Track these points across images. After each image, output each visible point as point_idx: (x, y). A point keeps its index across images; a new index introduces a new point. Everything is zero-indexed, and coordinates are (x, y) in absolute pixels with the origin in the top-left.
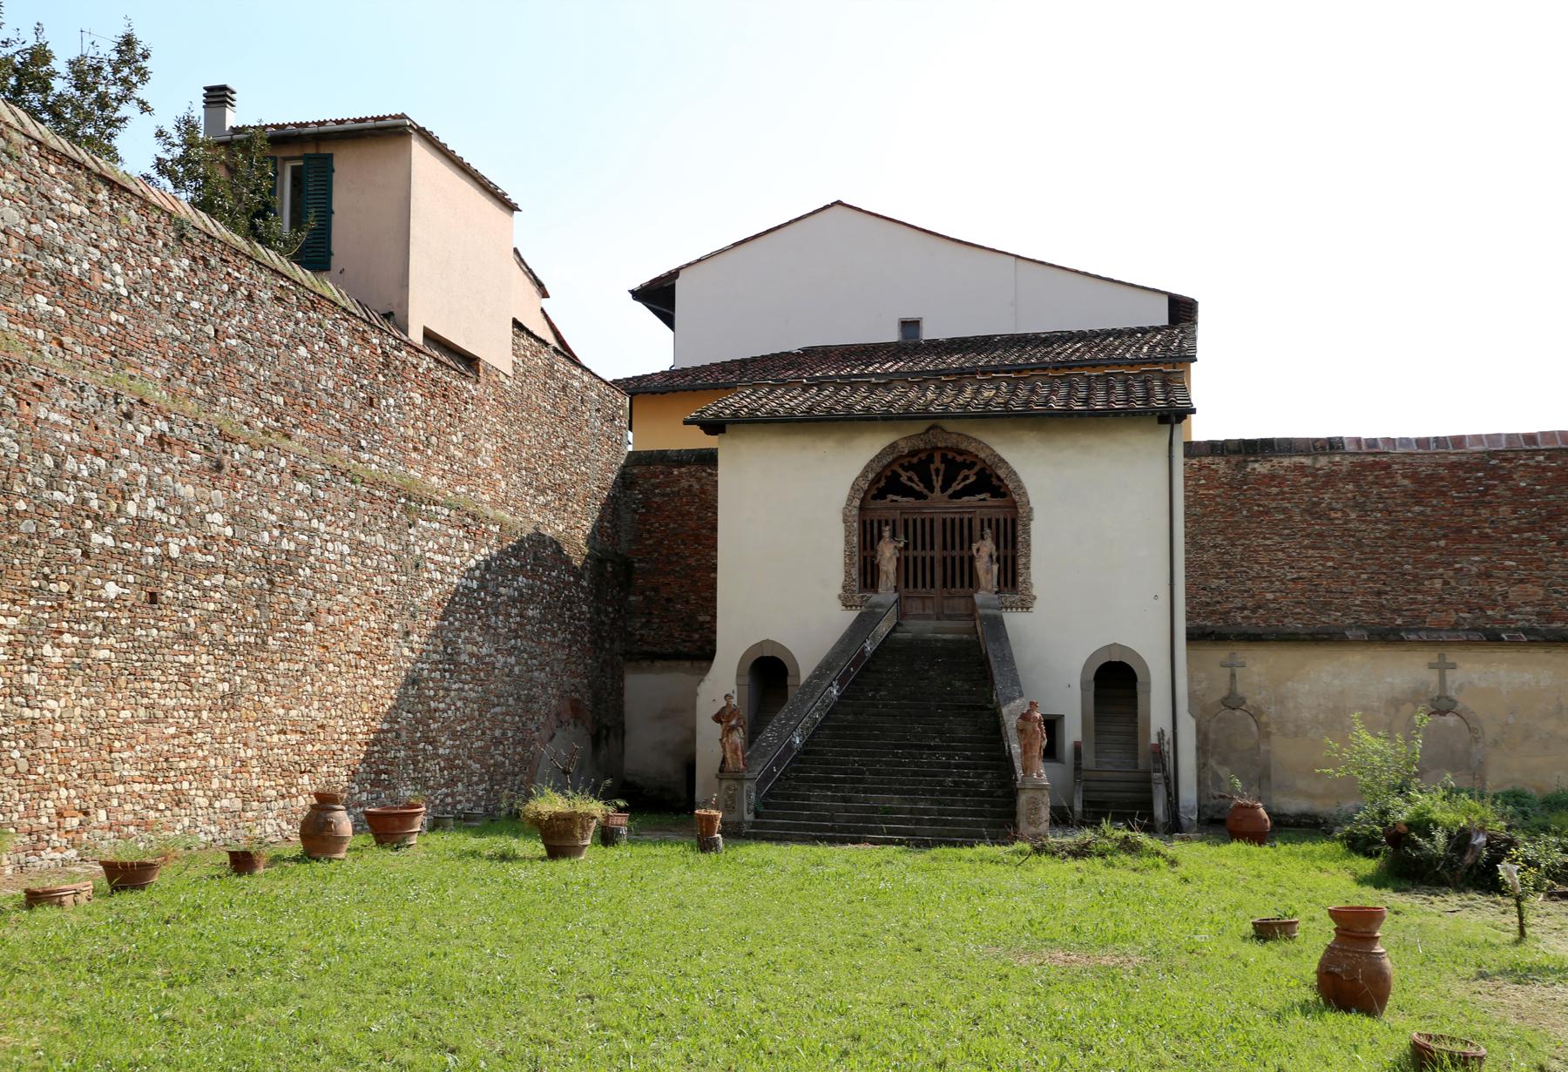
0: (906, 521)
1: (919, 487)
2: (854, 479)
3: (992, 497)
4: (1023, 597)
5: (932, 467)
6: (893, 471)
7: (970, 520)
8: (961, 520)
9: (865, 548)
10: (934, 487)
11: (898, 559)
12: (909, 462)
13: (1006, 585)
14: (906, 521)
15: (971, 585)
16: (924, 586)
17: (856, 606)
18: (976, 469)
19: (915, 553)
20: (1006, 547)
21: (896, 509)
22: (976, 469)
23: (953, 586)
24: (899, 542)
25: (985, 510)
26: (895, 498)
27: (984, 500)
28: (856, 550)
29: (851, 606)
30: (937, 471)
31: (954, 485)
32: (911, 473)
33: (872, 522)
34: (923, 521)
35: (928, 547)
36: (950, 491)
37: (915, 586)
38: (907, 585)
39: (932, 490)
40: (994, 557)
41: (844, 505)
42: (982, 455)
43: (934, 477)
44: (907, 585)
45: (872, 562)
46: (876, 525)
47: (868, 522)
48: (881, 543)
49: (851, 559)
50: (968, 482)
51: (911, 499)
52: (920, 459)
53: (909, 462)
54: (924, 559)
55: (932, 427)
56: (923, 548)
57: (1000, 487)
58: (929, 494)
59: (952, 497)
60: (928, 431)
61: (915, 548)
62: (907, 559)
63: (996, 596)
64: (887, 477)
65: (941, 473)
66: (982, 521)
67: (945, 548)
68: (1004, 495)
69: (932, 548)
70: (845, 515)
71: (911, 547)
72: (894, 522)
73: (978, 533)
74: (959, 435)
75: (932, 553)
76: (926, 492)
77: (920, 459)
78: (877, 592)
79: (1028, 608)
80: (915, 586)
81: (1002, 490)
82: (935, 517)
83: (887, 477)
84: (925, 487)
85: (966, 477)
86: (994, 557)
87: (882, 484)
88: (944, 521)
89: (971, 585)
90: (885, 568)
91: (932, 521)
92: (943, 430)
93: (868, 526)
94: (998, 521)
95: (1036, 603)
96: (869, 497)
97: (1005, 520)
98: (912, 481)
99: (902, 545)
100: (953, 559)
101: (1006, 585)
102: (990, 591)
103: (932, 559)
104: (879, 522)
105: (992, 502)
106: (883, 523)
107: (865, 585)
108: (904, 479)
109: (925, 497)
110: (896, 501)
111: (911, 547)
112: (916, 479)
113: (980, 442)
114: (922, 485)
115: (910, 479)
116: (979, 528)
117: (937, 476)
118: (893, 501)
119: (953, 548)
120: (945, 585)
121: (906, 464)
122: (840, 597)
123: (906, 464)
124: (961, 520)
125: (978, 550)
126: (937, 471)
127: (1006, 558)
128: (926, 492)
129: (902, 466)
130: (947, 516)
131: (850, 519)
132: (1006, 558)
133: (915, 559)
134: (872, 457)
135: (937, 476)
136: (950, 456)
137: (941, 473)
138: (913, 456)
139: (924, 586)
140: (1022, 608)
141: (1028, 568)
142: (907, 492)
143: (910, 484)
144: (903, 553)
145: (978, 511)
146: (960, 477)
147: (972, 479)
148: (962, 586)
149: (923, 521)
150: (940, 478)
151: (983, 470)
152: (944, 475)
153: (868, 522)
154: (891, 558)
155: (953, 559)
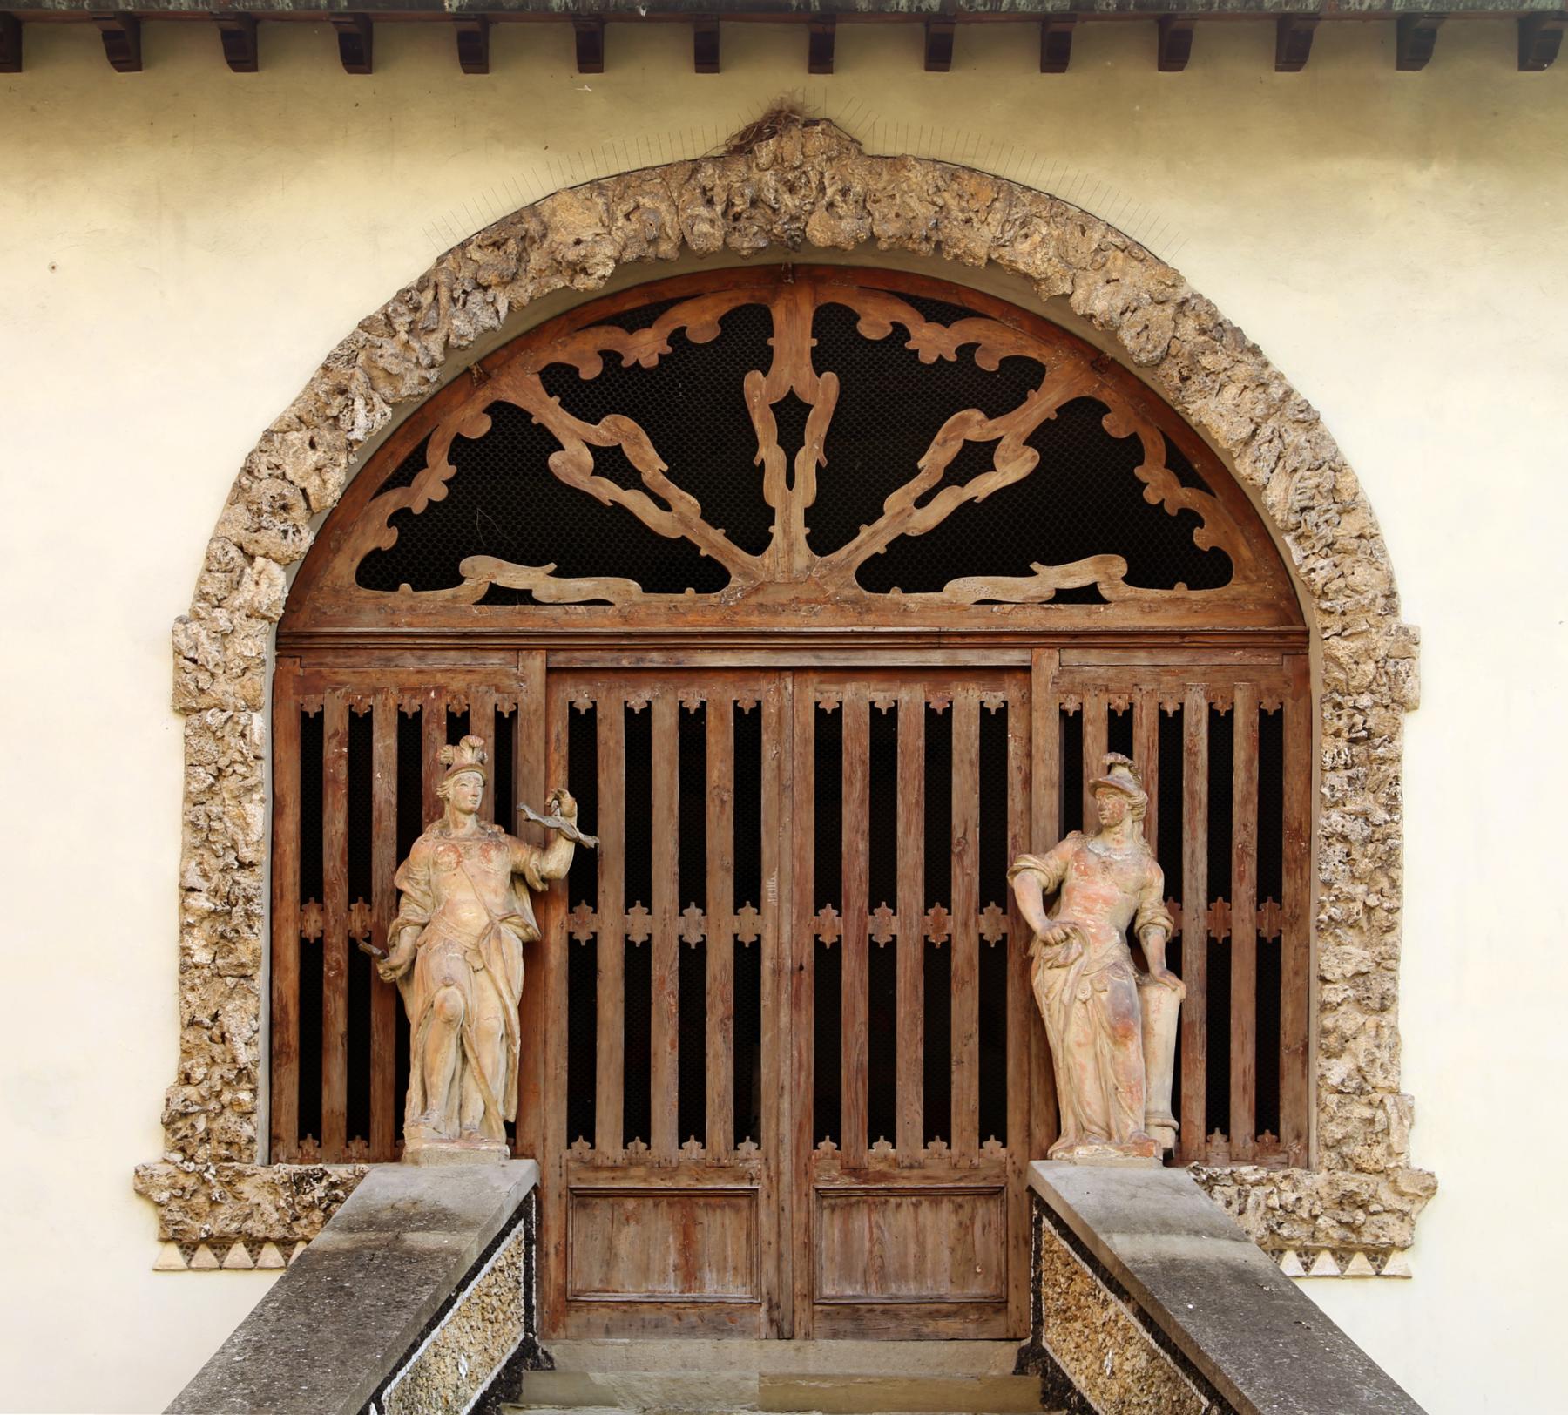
0: (583, 726)
2: (253, 440)
3: (1129, 579)
4: (1351, 1182)
5: (759, 391)
6: (500, 411)
7: (993, 725)
8: (938, 725)
9: (312, 887)
10: (769, 515)
11: (532, 951)
12: (610, 358)
13: (1218, 1118)
14: (583, 726)
15: (992, 1123)
16: (692, 1124)
17: (255, 1244)
18: (1041, 405)
19: (639, 924)
20: (1219, 886)
21: (516, 643)
22: (1041, 405)
23: (882, 1124)
24: (544, 844)
25: (1094, 662)
26: (514, 576)
27: (1089, 595)
28: (256, 883)
29: (219, 1244)
30: (791, 414)
31: (897, 501)
32: (618, 429)
33: (361, 727)
34: (692, 726)
35: (720, 884)
36: (872, 540)
37: (637, 1125)
38: (581, 1124)
40: (1155, 945)
41: (182, 599)
42: (1095, 298)
43: (770, 453)
44: (581, 1124)
45: (361, 967)
46: (385, 746)
47: (336, 724)
48: (423, 847)
49: (224, 942)
50: (983, 486)
51: (623, 590)
52: (678, 338)
53: (610, 358)
54: (693, 959)
55: (777, 122)
56: (693, 891)
57: (1190, 519)
58: (735, 557)
59: (875, 575)
60: (744, 145)
61: (639, 890)
62: (583, 958)
63: (1182, 1175)
64: (460, 449)
65: (816, 429)
66: (1072, 726)
67: (828, 889)
69: (748, 890)
70: (186, 659)
71: (612, 884)
72: (505, 727)
73: (1048, 801)
74: (955, 172)
75: (747, 924)
76: (713, 541)
77: (678, 338)
78: (394, 1151)
79: (1378, 1254)
80: (637, 1125)
81: (1202, 538)
82: (772, 697)
83: (460, 449)
84: (711, 516)
85: (976, 458)
86: (1155, 945)
87: (432, 486)
88: (828, 724)
89: (992, 1123)
90: (453, 999)
91: (748, 726)
92: (851, 145)
93: (335, 753)
94: (1171, 726)
95: (1432, 1222)
96: (344, 567)
97: (1221, 725)
98: (628, 477)
99: (559, 860)
100: (882, 959)
101: (1218, 1118)
102: (1142, 1146)
103: (747, 957)
104: (410, 730)
106: (435, 732)
107: (310, 1122)
109: (711, 577)
110: (525, 597)
111: (612, 884)
112: (649, 461)
113: (1086, 221)
114: (687, 504)
116: (1048, 768)
117: (791, 441)
118: (497, 595)
119: (883, 889)
120: (826, 1121)
121: (590, 370)
122: (143, 1184)
123: (590, 370)
124: (938, 725)
125: (1051, 899)
126: (791, 414)
127: (1219, 954)
128: (713, 541)
129: (559, 380)
130: (832, 695)
131: (223, 688)
132: (1219, 954)
133: (638, 958)
134: (373, 296)
135: (791, 441)
137: (816, 429)
139: (692, 1124)
140: (1342, 1253)
141: (1385, 1004)
143: (607, 491)
144: (559, 915)
145: (1047, 664)
146: (935, 458)
148: (937, 1125)
149: (692, 726)
150: (809, 458)
151: (1083, 412)
153: (336, 724)
154: (491, 932)
155: (882, 959)
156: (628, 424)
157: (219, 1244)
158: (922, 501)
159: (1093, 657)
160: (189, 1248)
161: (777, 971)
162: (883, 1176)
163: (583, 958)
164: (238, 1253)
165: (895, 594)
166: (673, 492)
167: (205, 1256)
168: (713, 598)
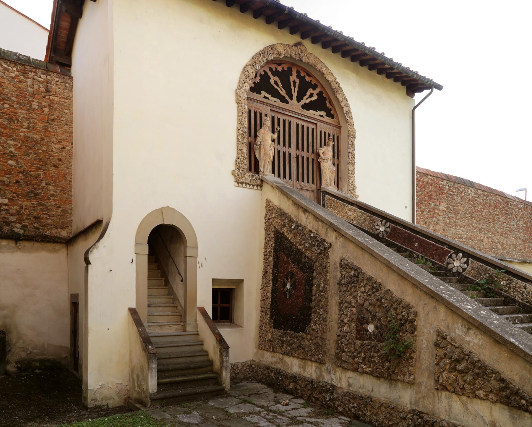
1: (283, 93)
30: (294, 82)
31: (305, 98)
39: (291, 98)
43: (292, 87)
68: (332, 117)
84: (287, 94)
85: (311, 95)
103: (290, 155)
105: (326, 119)
108: (272, 81)
109: (287, 102)
112: (280, 85)
114: (284, 91)
115: (276, 82)
117: (295, 87)
135: (295, 87)
136: (302, 74)
138: (279, 64)
142: (276, 94)
147: (315, 98)
150: (296, 89)
152: (298, 88)
156: (278, 78)
157: (242, 183)
158: (307, 99)
159: (323, 124)
160: (238, 183)
161: (293, 157)
162: (303, 187)
163: (279, 152)
164: (244, 185)
165: (305, 110)
166: (283, 89)
167: (240, 185)
168: (287, 105)
